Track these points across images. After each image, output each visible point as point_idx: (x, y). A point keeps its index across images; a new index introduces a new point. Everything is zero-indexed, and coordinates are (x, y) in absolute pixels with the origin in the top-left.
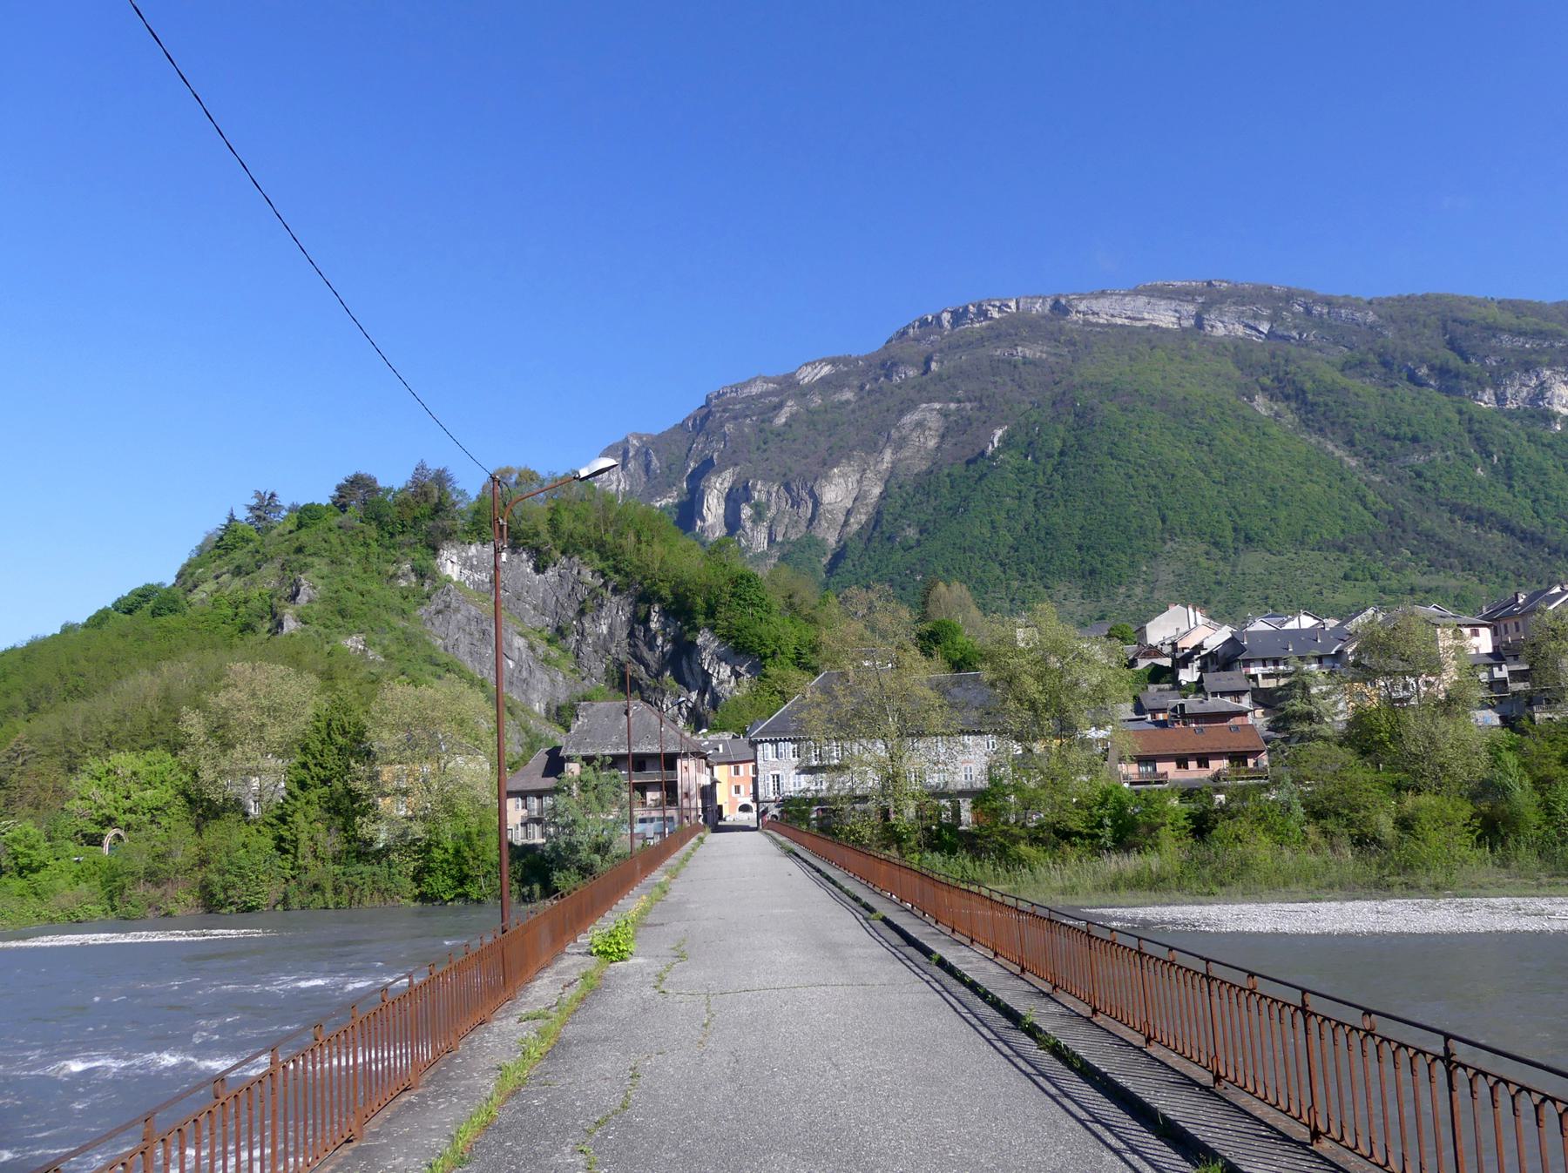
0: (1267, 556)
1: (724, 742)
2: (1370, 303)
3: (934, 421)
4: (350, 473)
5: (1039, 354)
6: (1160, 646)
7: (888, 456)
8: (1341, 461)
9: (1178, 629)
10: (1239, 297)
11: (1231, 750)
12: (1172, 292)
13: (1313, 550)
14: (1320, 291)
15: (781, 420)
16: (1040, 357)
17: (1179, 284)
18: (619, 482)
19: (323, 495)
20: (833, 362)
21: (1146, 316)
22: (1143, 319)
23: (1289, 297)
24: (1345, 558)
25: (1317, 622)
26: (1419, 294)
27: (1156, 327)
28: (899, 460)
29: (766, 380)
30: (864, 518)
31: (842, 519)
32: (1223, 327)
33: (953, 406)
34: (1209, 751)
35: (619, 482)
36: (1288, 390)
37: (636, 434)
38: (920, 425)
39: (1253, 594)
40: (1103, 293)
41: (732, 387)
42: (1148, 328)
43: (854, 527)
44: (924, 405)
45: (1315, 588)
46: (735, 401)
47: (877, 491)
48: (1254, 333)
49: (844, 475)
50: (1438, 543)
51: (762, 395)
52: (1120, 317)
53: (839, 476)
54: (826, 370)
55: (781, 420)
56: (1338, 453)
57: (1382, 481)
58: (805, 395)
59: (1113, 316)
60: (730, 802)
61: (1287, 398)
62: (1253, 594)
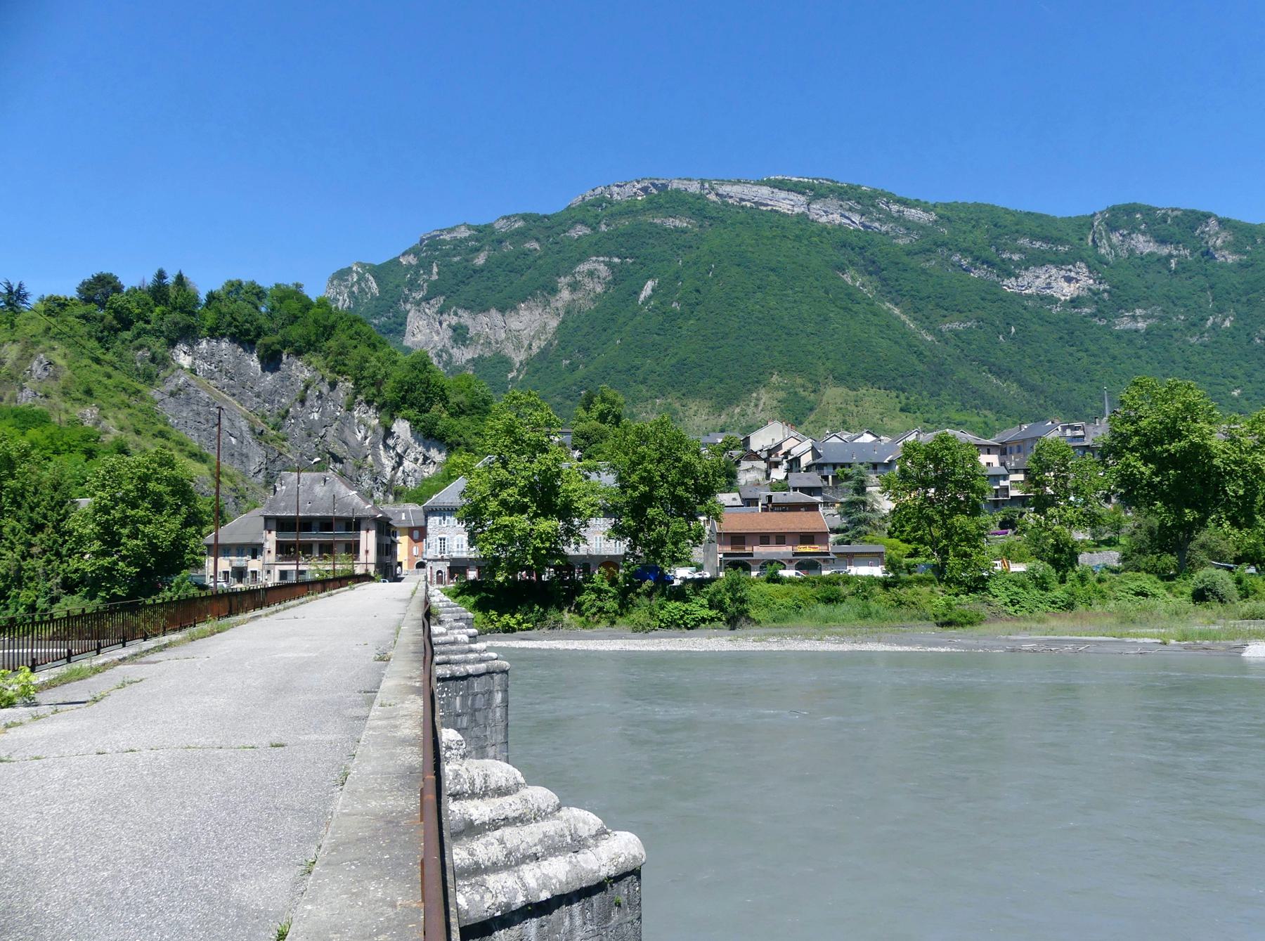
0: (847, 390)
1: (406, 512)
2: (935, 206)
3: (603, 270)
4: (96, 271)
5: (685, 225)
6: (759, 453)
7: (565, 295)
8: (904, 323)
9: (773, 440)
10: (843, 193)
11: (803, 531)
12: (791, 186)
13: (880, 389)
14: (899, 195)
15: (480, 260)
16: (687, 227)
17: (795, 179)
18: (345, 301)
19: (68, 289)
20: (524, 217)
21: (770, 203)
22: (767, 205)
23: (874, 196)
24: (902, 396)
25: (875, 438)
26: (970, 202)
27: (776, 211)
28: (574, 300)
29: (469, 227)
30: (543, 344)
31: (526, 343)
32: (828, 214)
33: (616, 260)
34: (786, 531)
35: (345, 301)
36: (873, 268)
37: (360, 263)
38: (591, 274)
39: (834, 419)
40: (739, 181)
41: (440, 230)
42: (772, 211)
43: (535, 350)
44: (594, 258)
45: (878, 416)
46: (444, 242)
47: (554, 323)
48: (849, 222)
49: (529, 309)
50: (968, 389)
51: (465, 239)
52: (749, 201)
53: (525, 310)
54: (520, 224)
55: (480, 260)
56: (903, 317)
57: (932, 341)
58: (501, 242)
59: (744, 200)
60: (409, 560)
61: (870, 274)
62: (834, 419)
